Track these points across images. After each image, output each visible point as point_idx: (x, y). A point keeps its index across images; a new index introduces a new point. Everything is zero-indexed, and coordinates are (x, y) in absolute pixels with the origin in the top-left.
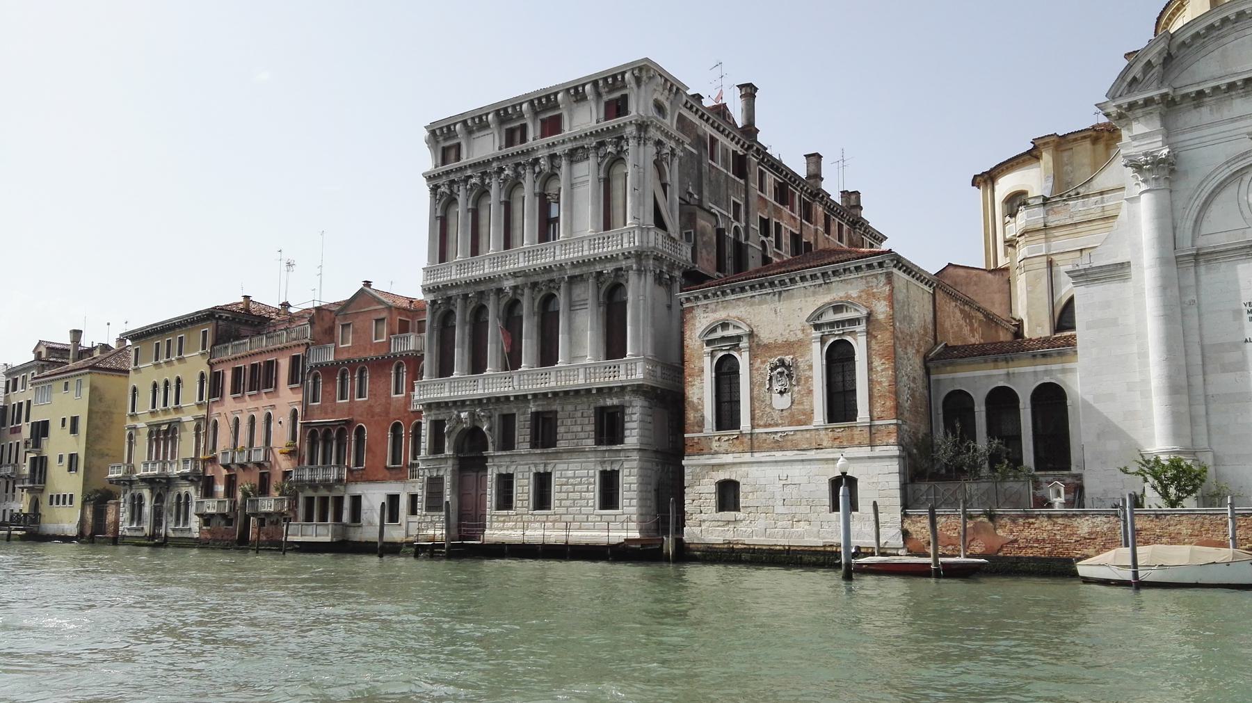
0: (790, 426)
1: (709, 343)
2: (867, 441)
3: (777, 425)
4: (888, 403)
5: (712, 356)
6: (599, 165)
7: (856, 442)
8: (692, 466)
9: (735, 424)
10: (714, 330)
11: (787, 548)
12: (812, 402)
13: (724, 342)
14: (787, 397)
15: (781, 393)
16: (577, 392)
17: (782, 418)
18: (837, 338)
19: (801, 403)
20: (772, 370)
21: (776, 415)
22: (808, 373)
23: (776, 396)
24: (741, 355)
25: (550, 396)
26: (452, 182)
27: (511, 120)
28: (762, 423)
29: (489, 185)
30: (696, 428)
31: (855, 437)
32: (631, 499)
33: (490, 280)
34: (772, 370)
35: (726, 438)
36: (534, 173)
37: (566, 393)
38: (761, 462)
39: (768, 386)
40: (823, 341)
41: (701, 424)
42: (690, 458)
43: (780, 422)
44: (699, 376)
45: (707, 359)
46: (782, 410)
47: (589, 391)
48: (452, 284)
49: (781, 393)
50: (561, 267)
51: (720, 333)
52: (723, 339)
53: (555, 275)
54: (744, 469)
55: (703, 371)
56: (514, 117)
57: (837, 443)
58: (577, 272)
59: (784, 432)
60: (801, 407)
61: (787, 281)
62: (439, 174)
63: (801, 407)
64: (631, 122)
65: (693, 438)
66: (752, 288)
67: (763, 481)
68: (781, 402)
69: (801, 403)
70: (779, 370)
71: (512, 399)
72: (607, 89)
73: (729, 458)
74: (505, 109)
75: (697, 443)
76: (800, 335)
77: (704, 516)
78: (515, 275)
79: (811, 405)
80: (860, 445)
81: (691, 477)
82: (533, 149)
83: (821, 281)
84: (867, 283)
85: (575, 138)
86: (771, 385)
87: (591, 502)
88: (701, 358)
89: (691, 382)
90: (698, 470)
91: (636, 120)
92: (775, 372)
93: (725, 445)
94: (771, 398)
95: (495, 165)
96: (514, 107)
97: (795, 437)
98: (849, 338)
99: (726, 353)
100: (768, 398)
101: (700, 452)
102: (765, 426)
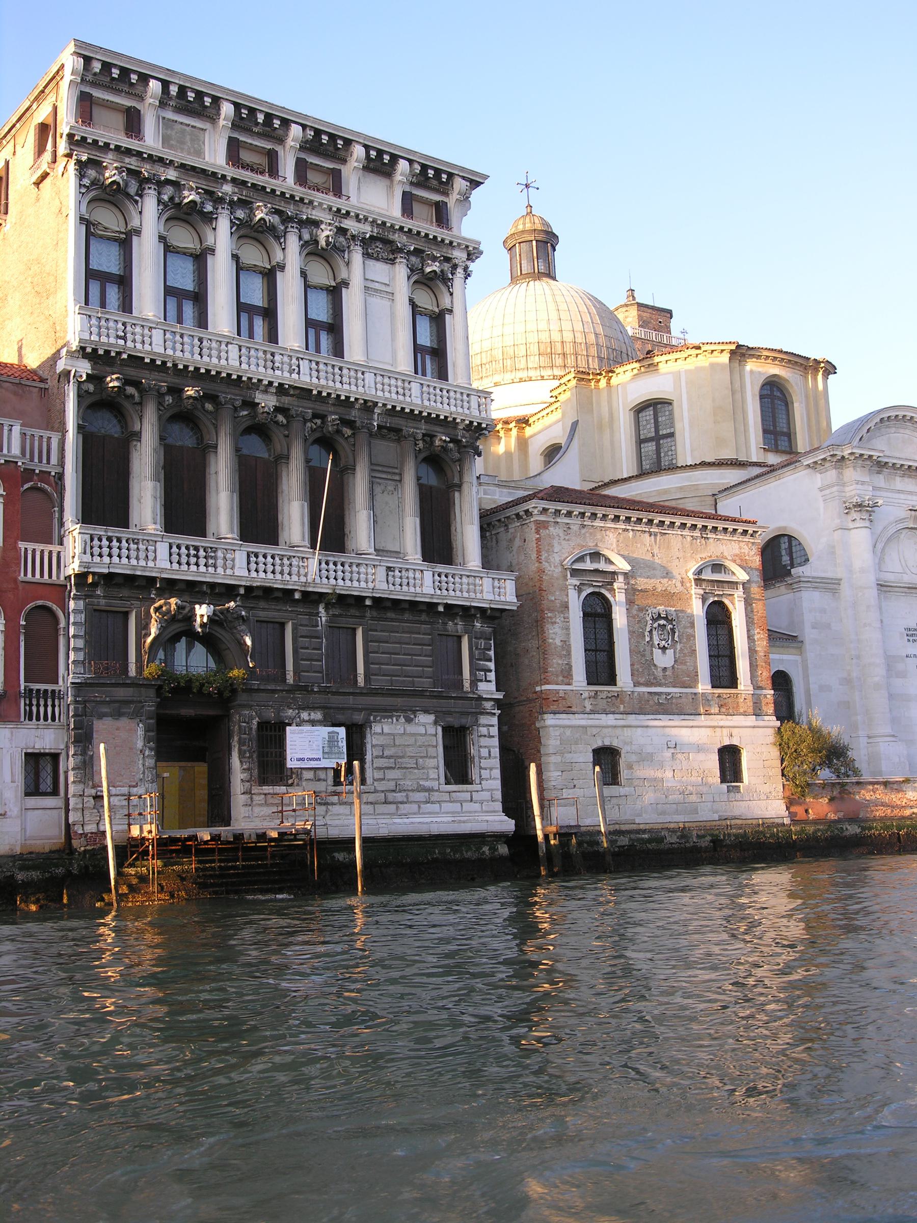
0: (674, 687)
1: (575, 573)
2: (751, 710)
3: (660, 685)
4: (764, 674)
5: (580, 591)
6: (409, 278)
7: (742, 710)
8: (560, 726)
9: (611, 679)
10: (581, 559)
11: (681, 825)
12: (696, 662)
13: (594, 576)
14: (670, 652)
15: (664, 649)
16: (413, 606)
17: (665, 677)
18: (716, 599)
19: (684, 663)
20: (654, 620)
21: (659, 673)
22: (690, 631)
23: (657, 652)
24: (614, 596)
25: (368, 602)
26: (134, 173)
27: (248, 131)
28: (642, 680)
29: (209, 219)
30: (561, 678)
31: (741, 705)
32: (491, 769)
33: (235, 382)
34: (654, 620)
35: (604, 695)
36: (300, 238)
37: (396, 604)
38: (647, 727)
39: (648, 639)
40: (704, 600)
41: (567, 675)
42: (558, 716)
43: (663, 681)
44: (562, 612)
45: (572, 594)
46: (665, 669)
47: (432, 606)
48: (153, 361)
49: (664, 649)
50: (368, 407)
51: (588, 565)
52: (596, 571)
53: (354, 414)
54: (627, 732)
55: (567, 607)
56: (256, 129)
57: (723, 710)
58: (389, 422)
59: (669, 694)
60: (684, 667)
61: (667, 523)
62: (107, 145)
63: (684, 667)
64: (467, 247)
65: (557, 691)
66: (628, 519)
67: (649, 749)
68: (663, 660)
69: (684, 663)
70: (662, 622)
71: (297, 596)
72: (414, 180)
73: (610, 720)
74: (252, 111)
75: (564, 698)
76: (679, 588)
77: (578, 792)
78: (282, 390)
79: (696, 667)
80: (745, 714)
81: (558, 742)
82: (311, 202)
83: (697, 533)
84: (740, 548)
85: (384, 223)
86: (651, 638)
87: (433, 774)
88: (565, 589)
89: (550, 617)
90: (568, 732)
91: (474, 248)
92: (656, 625)
93: (602, 704)
94: (652, 653)
95: (228, 188)
96: (269, 117)
97: (680, 701)
98: (726, 601)
99: (597, 590)
100: (647, 653)
101: (568, 710)
102: (648, 684)
